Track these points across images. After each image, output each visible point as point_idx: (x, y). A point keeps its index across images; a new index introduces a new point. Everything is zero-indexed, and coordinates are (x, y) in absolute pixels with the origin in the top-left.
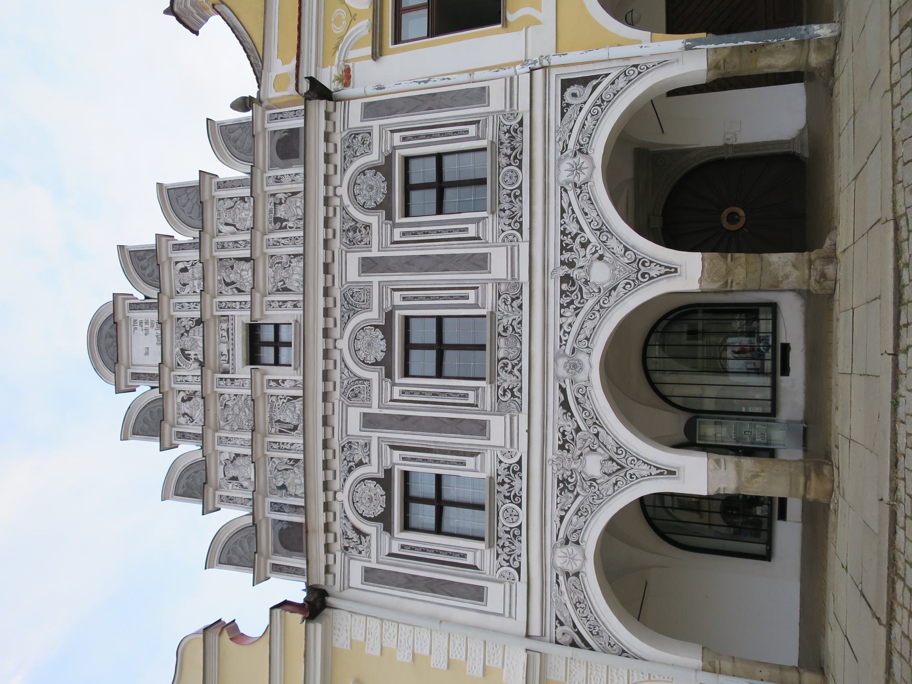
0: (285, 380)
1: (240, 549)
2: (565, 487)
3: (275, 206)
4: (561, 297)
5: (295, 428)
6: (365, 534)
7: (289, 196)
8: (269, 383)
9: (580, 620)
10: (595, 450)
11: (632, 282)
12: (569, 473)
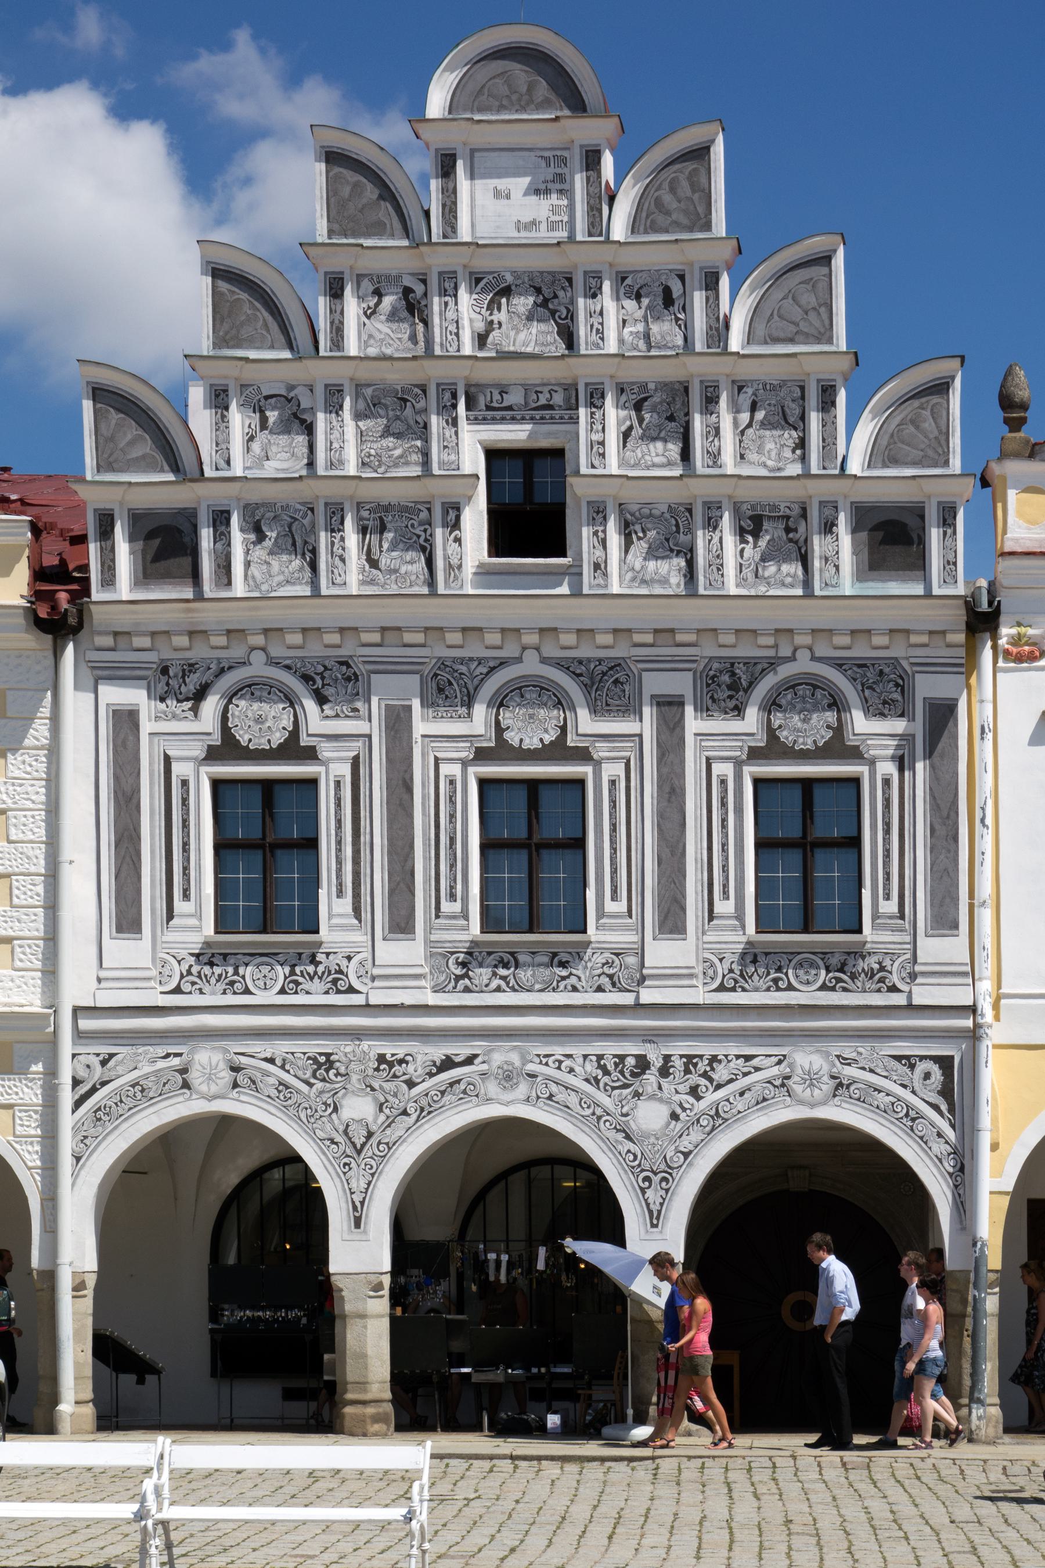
0: (460, 545)
1: (129, 437)
2: (320, 1065)
3: (783, 517)
4: (615, 1056)
5: (374, 563)
6: (198, 708)
7: (800, 549)
8: (453, 508)
9: (117, 1092)
10: (381, 1110)
11: (637, 1163)
12: (342, 1070)
